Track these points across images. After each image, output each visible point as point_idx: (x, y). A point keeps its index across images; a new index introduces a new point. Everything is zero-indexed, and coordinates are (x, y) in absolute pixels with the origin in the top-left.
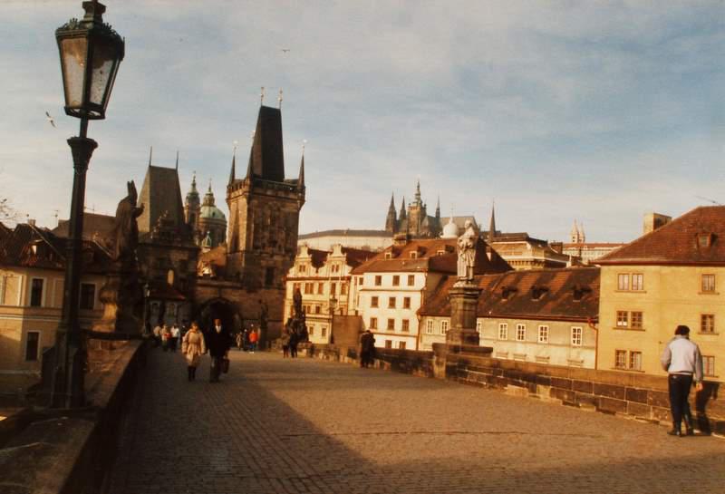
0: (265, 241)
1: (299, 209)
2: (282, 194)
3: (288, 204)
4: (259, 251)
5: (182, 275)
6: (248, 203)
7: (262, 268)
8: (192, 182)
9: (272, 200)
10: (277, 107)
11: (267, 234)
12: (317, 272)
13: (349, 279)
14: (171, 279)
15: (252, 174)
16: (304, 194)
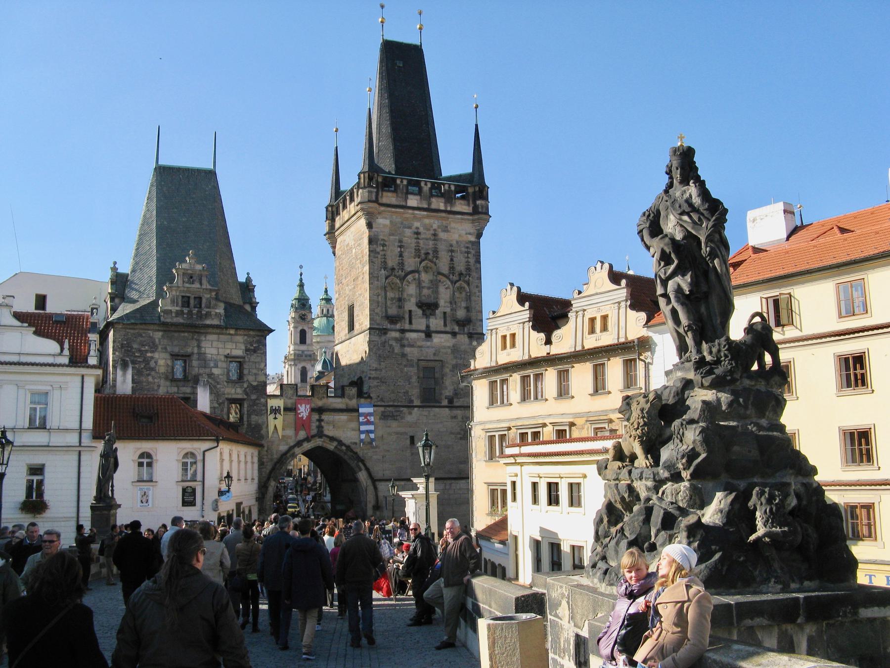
0: (411, 305)
1: (479, 235)
2: (439, 203)
3: (453, 225)
4: (398, 326)
5: (237, 392)
6: (369, 225)
7: (410, 364)
8: (298, 282)
9: (419, 219)
10: (414, 40)
11: (411, 290)
12: (548, 342)
13: (644, 344)
14: (204, 402)
15: (372, 170)
16: (486, 198)
